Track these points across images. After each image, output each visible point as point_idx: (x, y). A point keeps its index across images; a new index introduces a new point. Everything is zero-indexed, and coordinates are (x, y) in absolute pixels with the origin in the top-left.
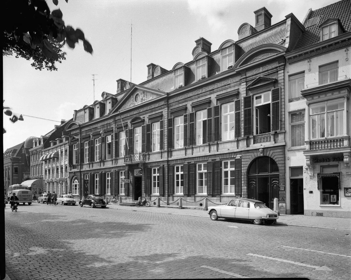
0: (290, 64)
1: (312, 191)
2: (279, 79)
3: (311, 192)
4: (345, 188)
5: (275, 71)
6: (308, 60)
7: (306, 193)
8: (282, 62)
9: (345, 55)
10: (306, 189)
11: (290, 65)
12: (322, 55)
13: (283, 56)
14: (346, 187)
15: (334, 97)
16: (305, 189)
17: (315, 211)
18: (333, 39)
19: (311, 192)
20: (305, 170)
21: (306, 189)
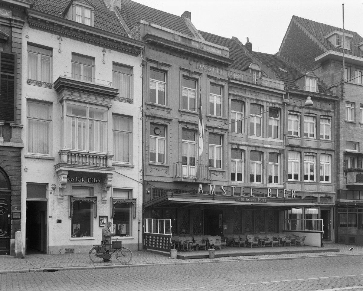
0: (31, 26)
1: (61, 220)
2: (14, 40)
3: (59, 221)
4: (100, 217)
5: (6, 24)
6: (59, 36)
7: (51, 224)
8: (19, 17)
9: (102, 56)
10: (52, 217)
11: (31, 27)
12: (76, 40)
13: (25, 8)
14: (101, 215)
15: (88, 100)
16: (51, 217)
17: (65, 246)
18: (85, 26)
19: (59, 221)
20: (52, 189)
21: (52, 217)
